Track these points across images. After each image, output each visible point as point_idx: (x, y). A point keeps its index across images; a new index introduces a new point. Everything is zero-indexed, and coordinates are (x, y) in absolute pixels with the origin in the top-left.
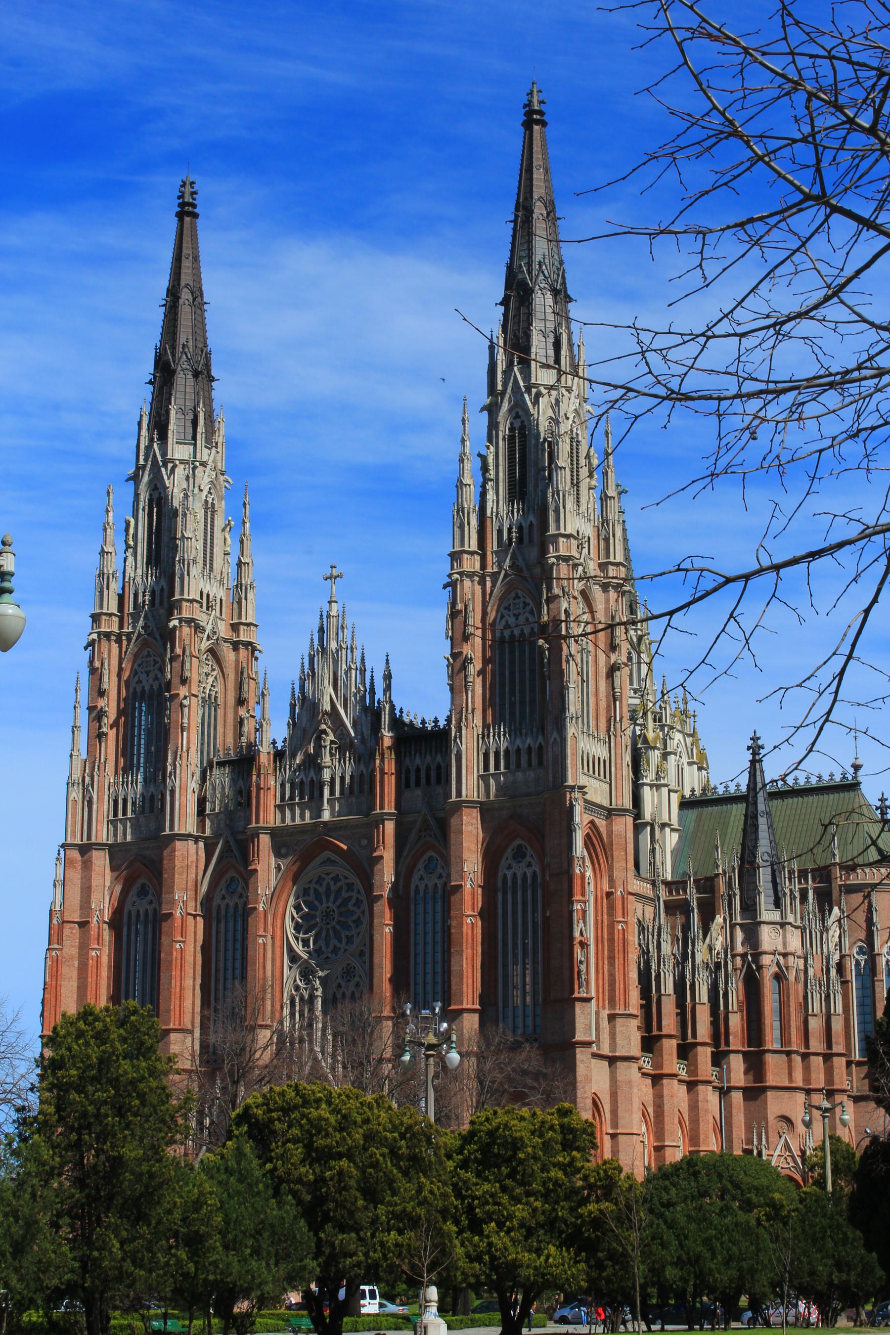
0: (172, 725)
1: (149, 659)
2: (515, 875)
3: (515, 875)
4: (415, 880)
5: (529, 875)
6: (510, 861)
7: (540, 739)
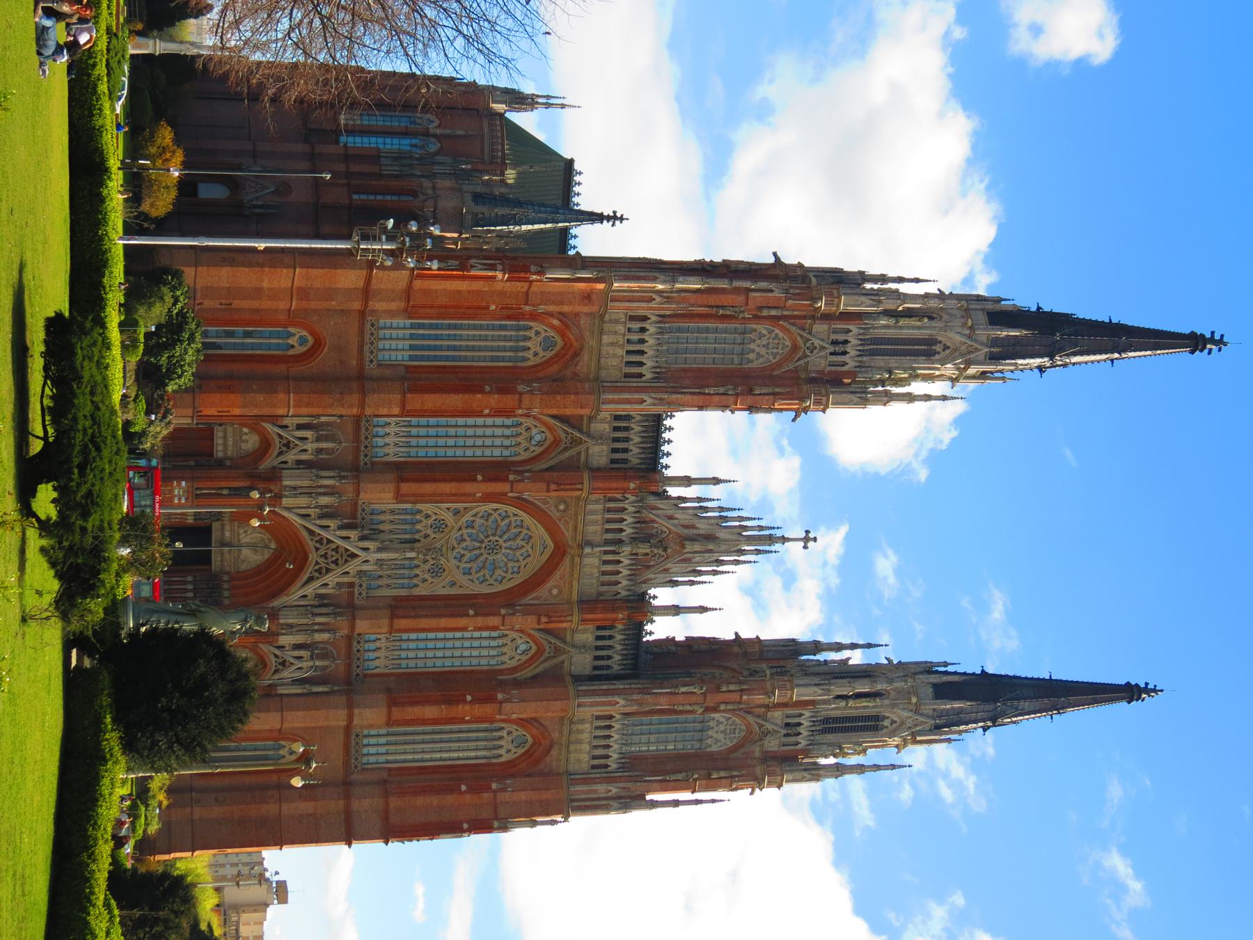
0: (708, 397)
1: (781, 346)
2: (501, 738)
3: (501, 738)
4: (515, 635)
5: (502, 751)
6: (515, 734)
7: (614, 766)
